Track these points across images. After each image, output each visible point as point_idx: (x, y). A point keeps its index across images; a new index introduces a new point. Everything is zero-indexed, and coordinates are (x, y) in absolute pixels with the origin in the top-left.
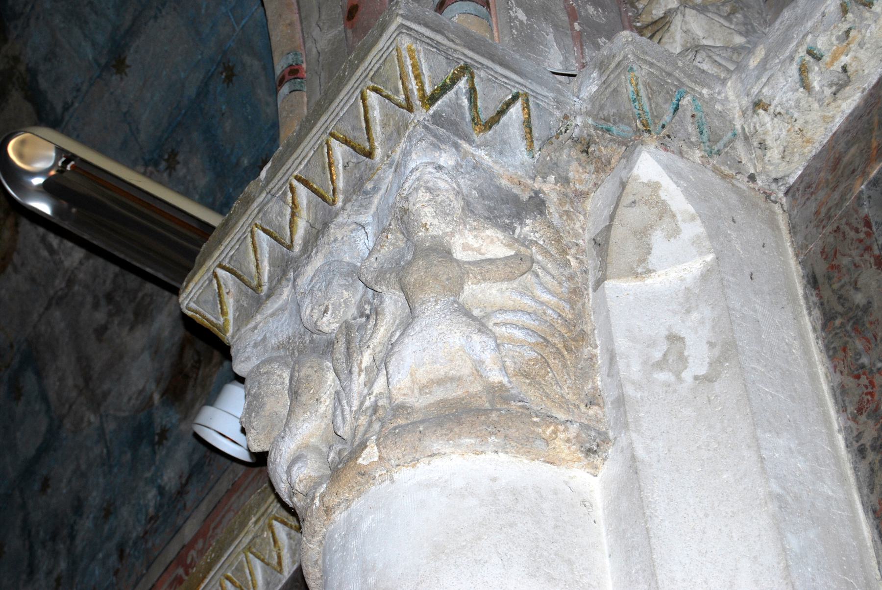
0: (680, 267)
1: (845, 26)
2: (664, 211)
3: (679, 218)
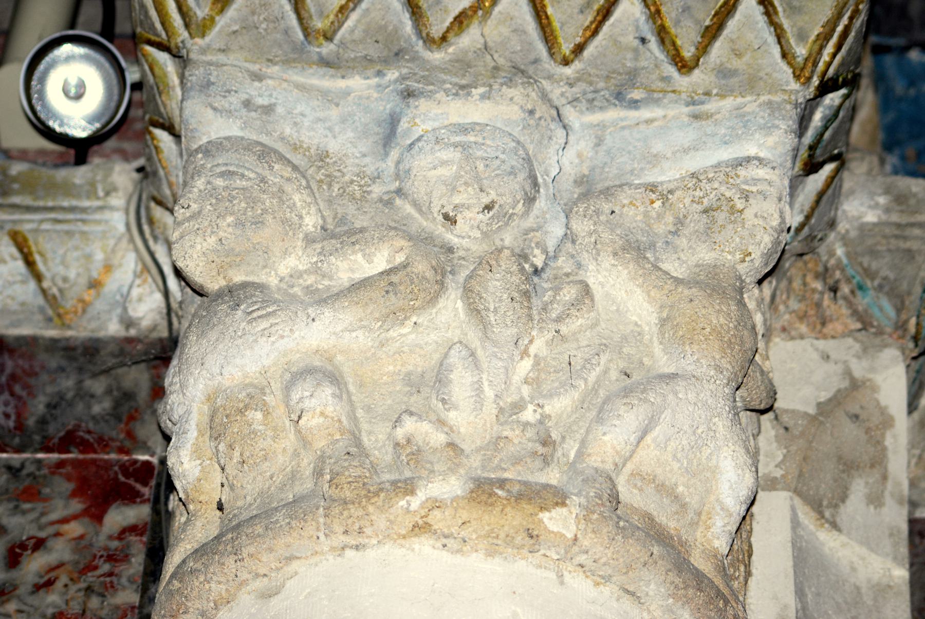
0: (864, 551)
2: (878, 461)
3: (890, 485)
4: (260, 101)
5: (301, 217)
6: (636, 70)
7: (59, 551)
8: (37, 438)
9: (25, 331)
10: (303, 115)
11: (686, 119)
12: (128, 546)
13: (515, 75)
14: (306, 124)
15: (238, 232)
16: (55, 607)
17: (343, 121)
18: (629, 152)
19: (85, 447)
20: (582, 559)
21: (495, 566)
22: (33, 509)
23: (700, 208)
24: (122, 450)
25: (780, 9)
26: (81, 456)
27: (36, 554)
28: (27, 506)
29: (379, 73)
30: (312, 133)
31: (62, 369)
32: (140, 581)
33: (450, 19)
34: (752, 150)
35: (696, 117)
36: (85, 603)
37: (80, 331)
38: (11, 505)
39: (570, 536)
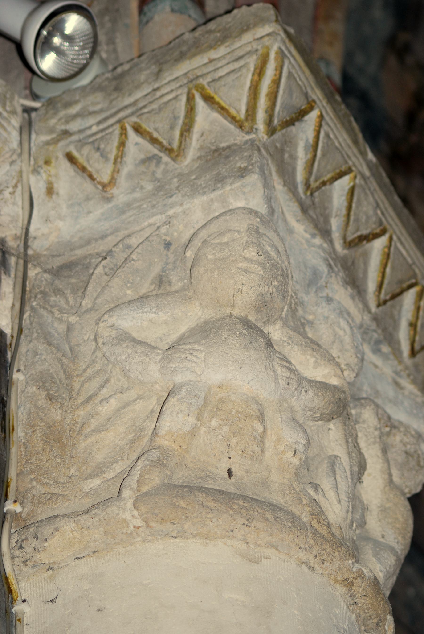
11: (390, 380)
23: (404, 449)
29: (313, 236)
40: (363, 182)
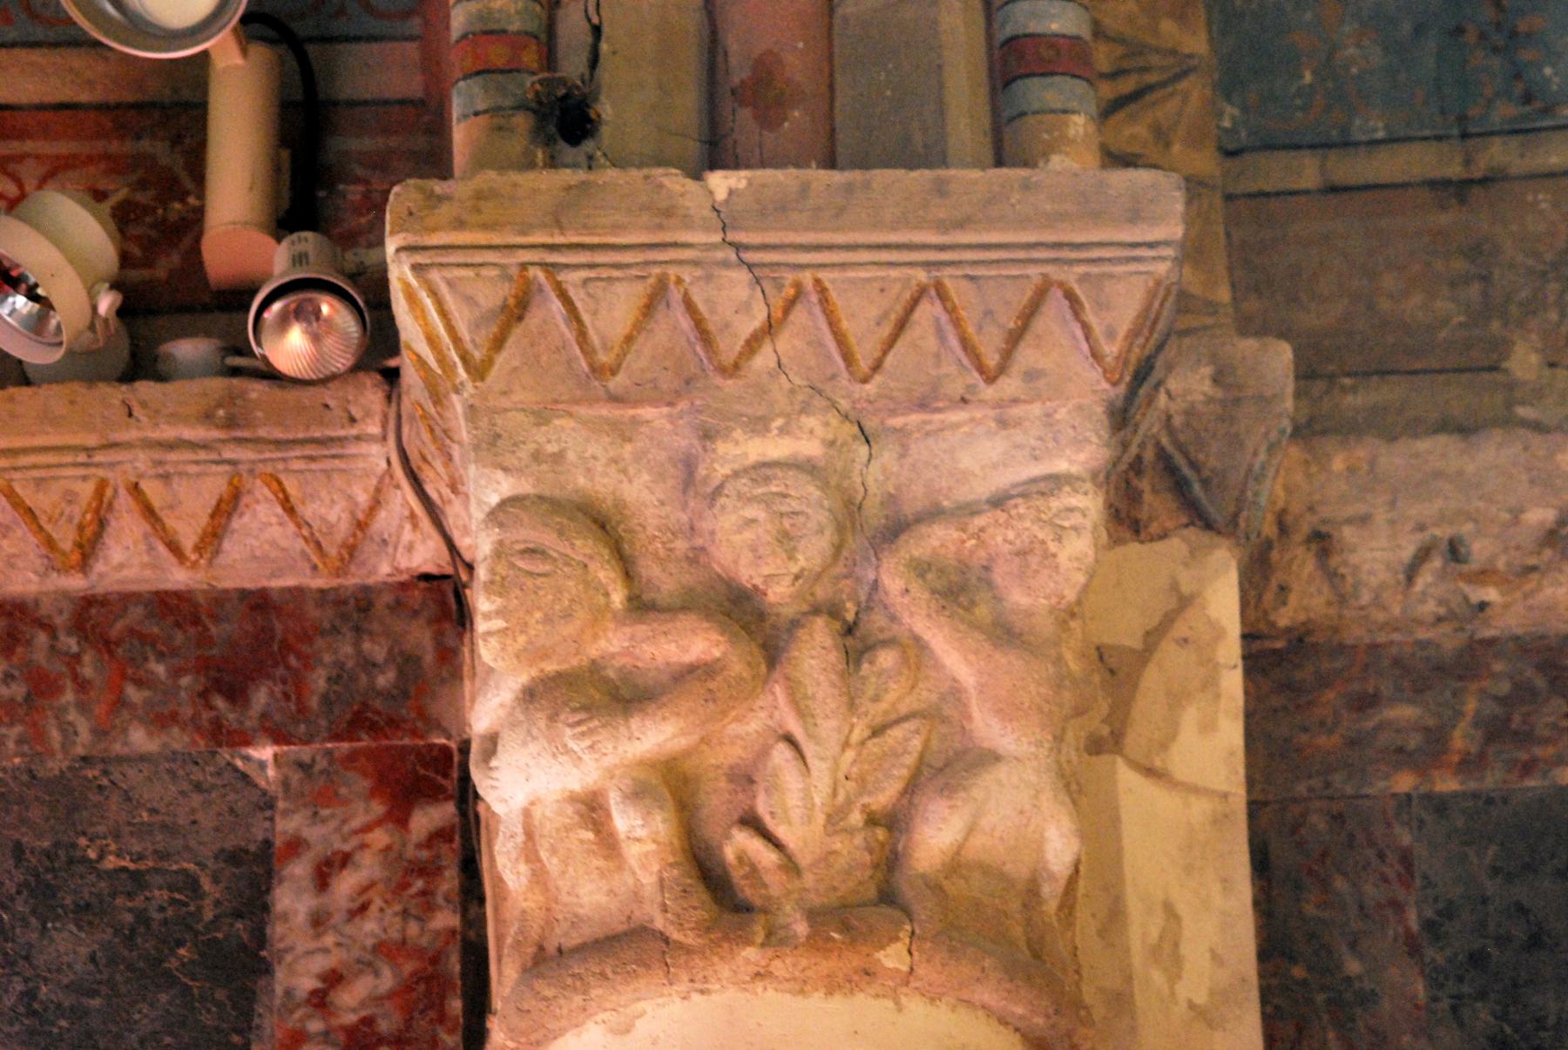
1: (1532, 561)
3: (1223, 701)
4: (552, 448)
5: (607, 595)
6: (939, 378)
7: (367, 868)
8: (323, 723)
9: (290, 581)
10: (594, 458)
11: (993, 425)
12: (438, 857)
13: (812, 397)
14: (600, 469)
15: (548, 628)
16: (375, 936)
17: (638, 457)
18: (936, 467)
19: (374, 729)
20: (918, 984)
21: (837, 1003)
22: (333, 816)
24: (414, 733)
25: (1087, 305)
26: (374, 745)
27: (345, 872)
28: (325, 812)
29: (670, 404)
30: (606, 480)
31: (335, 630)
32: (457, 899)
33: (742, 343)
34: (1061, 466)
35: (1003, 423)
36: (404, 930)
37: (352, 580)
38: (309, 813)
39: (905, 968)
40: (698, 272)
